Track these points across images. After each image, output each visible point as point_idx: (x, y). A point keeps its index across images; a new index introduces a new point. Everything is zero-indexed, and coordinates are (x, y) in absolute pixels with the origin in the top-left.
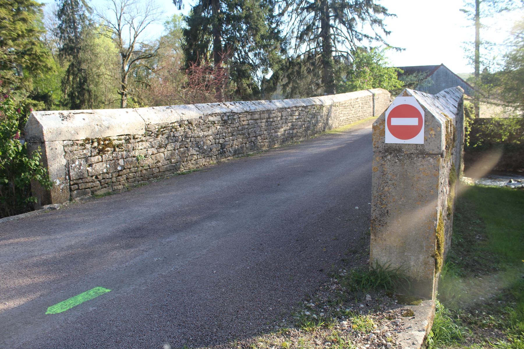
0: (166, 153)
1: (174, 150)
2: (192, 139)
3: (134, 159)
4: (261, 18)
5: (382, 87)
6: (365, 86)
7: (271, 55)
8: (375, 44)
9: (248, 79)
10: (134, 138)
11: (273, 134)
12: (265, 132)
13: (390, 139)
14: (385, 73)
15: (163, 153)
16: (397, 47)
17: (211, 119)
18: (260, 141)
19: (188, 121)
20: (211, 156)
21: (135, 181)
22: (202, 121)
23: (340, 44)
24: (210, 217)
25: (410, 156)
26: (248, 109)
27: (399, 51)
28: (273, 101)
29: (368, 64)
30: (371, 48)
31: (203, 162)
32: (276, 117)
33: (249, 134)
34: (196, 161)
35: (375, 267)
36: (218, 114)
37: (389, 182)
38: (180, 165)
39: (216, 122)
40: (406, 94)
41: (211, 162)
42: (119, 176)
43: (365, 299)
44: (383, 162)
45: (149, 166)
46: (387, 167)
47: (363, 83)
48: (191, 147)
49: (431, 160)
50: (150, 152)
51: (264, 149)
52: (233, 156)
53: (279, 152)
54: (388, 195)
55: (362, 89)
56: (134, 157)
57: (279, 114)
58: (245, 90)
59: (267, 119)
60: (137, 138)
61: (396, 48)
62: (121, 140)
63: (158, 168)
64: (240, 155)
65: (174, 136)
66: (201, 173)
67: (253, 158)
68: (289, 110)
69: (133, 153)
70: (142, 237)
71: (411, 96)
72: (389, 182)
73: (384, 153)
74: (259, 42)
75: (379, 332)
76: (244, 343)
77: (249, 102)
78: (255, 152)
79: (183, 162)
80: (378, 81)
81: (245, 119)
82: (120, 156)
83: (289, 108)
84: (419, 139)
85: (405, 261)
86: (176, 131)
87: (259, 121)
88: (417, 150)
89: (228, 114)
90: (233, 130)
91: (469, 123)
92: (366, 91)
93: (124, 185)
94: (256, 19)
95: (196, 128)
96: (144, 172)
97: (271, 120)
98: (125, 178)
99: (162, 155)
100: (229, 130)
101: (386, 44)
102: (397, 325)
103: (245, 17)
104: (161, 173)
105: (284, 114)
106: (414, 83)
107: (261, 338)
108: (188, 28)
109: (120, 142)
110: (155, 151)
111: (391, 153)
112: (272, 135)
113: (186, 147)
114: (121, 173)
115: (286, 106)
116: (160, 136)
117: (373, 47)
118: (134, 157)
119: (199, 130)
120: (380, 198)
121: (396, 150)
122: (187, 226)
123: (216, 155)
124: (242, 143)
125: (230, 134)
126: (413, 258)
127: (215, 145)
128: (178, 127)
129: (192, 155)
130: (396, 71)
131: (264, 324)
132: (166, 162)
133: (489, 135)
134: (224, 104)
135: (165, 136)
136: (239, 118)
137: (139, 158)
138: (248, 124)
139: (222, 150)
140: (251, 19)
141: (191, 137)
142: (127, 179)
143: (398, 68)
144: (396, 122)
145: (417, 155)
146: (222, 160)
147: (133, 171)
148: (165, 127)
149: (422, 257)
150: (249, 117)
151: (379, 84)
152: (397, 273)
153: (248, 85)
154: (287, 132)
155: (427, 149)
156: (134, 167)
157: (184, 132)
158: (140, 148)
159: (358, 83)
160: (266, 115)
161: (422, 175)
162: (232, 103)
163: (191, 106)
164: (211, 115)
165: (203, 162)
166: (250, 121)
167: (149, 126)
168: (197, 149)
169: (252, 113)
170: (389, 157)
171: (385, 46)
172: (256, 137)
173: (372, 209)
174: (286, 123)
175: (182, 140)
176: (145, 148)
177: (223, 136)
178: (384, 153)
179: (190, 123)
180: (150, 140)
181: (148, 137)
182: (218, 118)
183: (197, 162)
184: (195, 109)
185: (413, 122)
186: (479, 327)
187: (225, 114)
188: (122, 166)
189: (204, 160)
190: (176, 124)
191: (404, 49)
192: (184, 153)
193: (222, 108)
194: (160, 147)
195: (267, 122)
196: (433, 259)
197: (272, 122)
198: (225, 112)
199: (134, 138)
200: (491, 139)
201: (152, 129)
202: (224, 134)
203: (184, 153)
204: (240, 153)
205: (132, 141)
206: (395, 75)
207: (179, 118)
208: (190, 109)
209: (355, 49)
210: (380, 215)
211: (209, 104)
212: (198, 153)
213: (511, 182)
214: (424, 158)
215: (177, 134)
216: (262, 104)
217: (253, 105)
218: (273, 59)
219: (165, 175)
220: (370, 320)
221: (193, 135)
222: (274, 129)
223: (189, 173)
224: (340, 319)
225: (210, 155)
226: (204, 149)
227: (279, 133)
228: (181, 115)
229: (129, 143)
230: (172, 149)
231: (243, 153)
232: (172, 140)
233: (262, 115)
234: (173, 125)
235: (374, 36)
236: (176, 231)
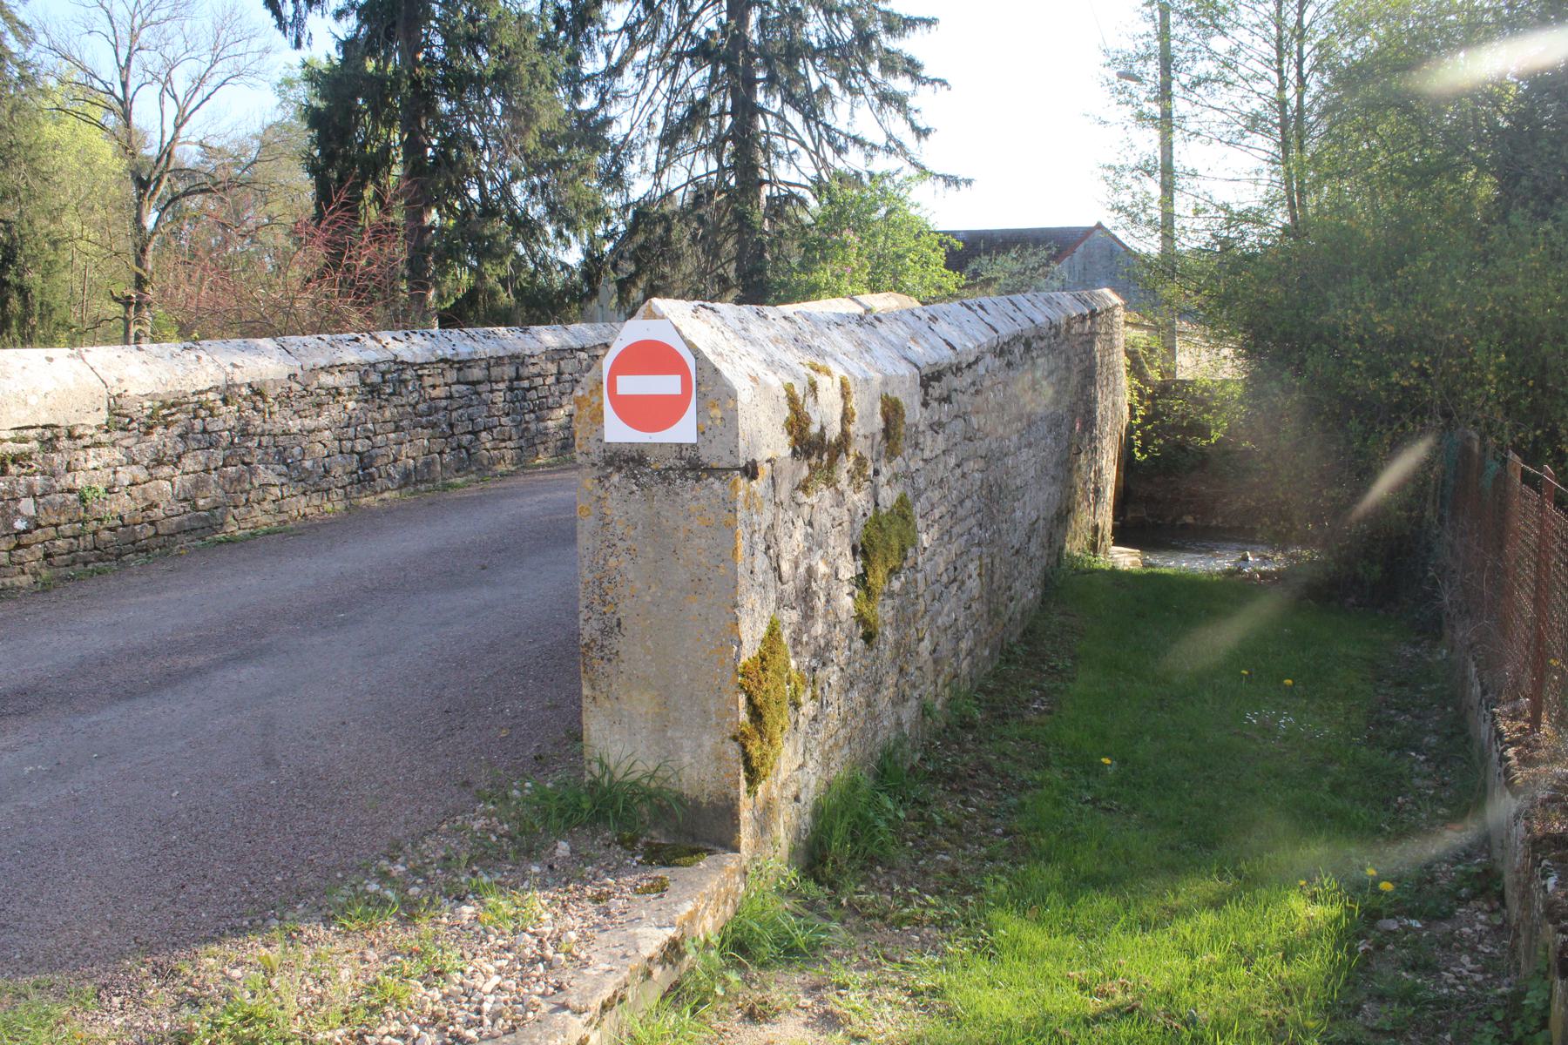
0: (177, 480)
1: (207, 471)
2: (265, 440)
3: (72, 497)
4: (542, 82)
5: (900, 291)
6: (844, 283)
7: (571, 193)
8: (881, 163)
9: (502, 263)
10: (70, 436)
11: (533, 426)
12: (504, 420)
13: (617, 431)
14: (909, 250)
15: (169, 479)
17: (327, 380)
18: (488, 445)
19: (250, 386)
21: (74, 562)
22: (296, 387)
23: (783, 163)
24: (243, 658)
25: (664, 476)
26: (449, 353)
28: (534, 329)
29: (861, 225)
30: (872, 175)
31: (300, 505)
32: (539, 375)
33: (451, 426)
34: (274, 500)
35: (597, 772)
36: (352, 367)
37: (619, 544)
39: (345, 390)
40: (652, 315)
41: (328, 507)
42: (18, 546)
43: (552, 854)
44: (601, 493)
45: (121, 518)
46: (614, 506)
47: (838, 277)
48: (260, 462)
49: (717, 485)
50: (125, 476)
51: (501, 468)
52: (400, 488)
53: (549, 477)
55: (835, 293)
56: (71, 491)
57: (553, 368)
58: (493, 294)
59: (511, 381)
60: (80, 437)
62: (25, 440)
63: (152, 523)
64: (422, 487)
65: (204, 431)
66: (289, 536)
67: (454, 494)
68: (583, 355)
69: (66, 481)
70: (22, 713)
71: (663, 317)
72: (619, 544)
74: (535, 153)
75: (548, 930)
76: (161, 959)
77: (456, 331)
78: (473, 476)
79: (236, 507)
80: (884, 272)
81: (440, 381)
82: (21, 489)
83: (582, 349)
84: (684, 431)
85: (669, 752)
87: (481, 388)
89: (383, 367)
91: (1141, 394)
92: (846, 301)
93: (35, 574)
94: (526, 83)
95: (276, 408)
96: (106, 535)
97: (526, 384)
98: (40, 554)
99: (166, 487)
100: (388, 414)
101: (915, 165)
102: (607, 914)
103: (494, 78)
104: (161, 540)
105: (568, 366)
106: (995, 279)
107: (215, 948)
108: (318, 103)
109: (25, 447)
110: (142, 475)
111: (619, 469)
112: (527, 429)
113: (244, 463)
114: (25, 539)
115: (575, 344)
116: (160, 429)
117: (878, 172)
118: (71, 491)
119: (288, 412)
120: (600, 586)
121: (633, 459)
122: (170, 680)
123: (343, 487)
124: (430, 452)
125: (391, 426)
126: (687, 744)
127: (339, 458)
128: (219, 403)
129: (265, 486)
130: (941, 243)
131: (240, 916)
132: (178, 507)
133: (1176, 428)
134: (373, 338)
135: (175, 430)
136: (420, 377)
137: (89, 495)
138: (450, 397)
139: (365, 472)
140: (512, 84)
142: (47, 556)
143: (946, 233)
144: (629, 385)
145: (682, 474)
146: (364, 501)
147: (69, 533)
148: (173, 405)
149: (708, 742)
150: (452, 376)
152: (653, 785)
153: (503, 281)
155: (708, 456)
156: (70, 521)
157: (239, 419)
158: (91, 464)
159: (823, 275)
160: (509, 371)
162: (400, 334)
163: (266, 343)
164: (328, 369)
165: (300, 505)
166: (454, 388)
167: (120, 402)
168: (282, 468)
169: (462, 365)
170: (616, 478)
171: (914, 172)
172: (475, 433)
173: (582, 617)
175: (232, 443)
176: (109, 466)
178: (603, 469)
179: (257, 392)
180: (125, 443)
181: (118, 434)
182: (352, 378)
185: (669, 385)
186: (889, 926)
187: (373, 365)
188: (29, 519)
189: (304, 500)
190: (211, 396)
191: (969, 182)
192: (239, 479)
193: (364, 348)
194: (159, 462)
195: (511, 389)
196: (735, 745)
197: (529, 390)
198: (372, 360)
199: (70, 436)
200: (1183, 439)
201: (133, 409)
202: (370, 426)
204: (421, 482)
205: (64, 443)
206: (939, 257)
207: (223, 377)
208: (259, 352)
209: (826, 178)
210: (602, 632)
211: (326, 337)
212: (284, 480)
213: (1245, 559)
214: (698, 479)
217: (469, 342)
218: (577, 205)
219: (175, 544)
220: (538, 902)
221: (267, 427)
222: (533, 411)
224: (461, 900)
225: (325, 485)
226: (305, 469)
227: (550, 424)
228: (229, 369)
229: (55, 449)
230: (197, 468)
231: (434, 481)
232: (199, 441)
233: (495, 372)
235: (881, 140)
236: (130, 695)
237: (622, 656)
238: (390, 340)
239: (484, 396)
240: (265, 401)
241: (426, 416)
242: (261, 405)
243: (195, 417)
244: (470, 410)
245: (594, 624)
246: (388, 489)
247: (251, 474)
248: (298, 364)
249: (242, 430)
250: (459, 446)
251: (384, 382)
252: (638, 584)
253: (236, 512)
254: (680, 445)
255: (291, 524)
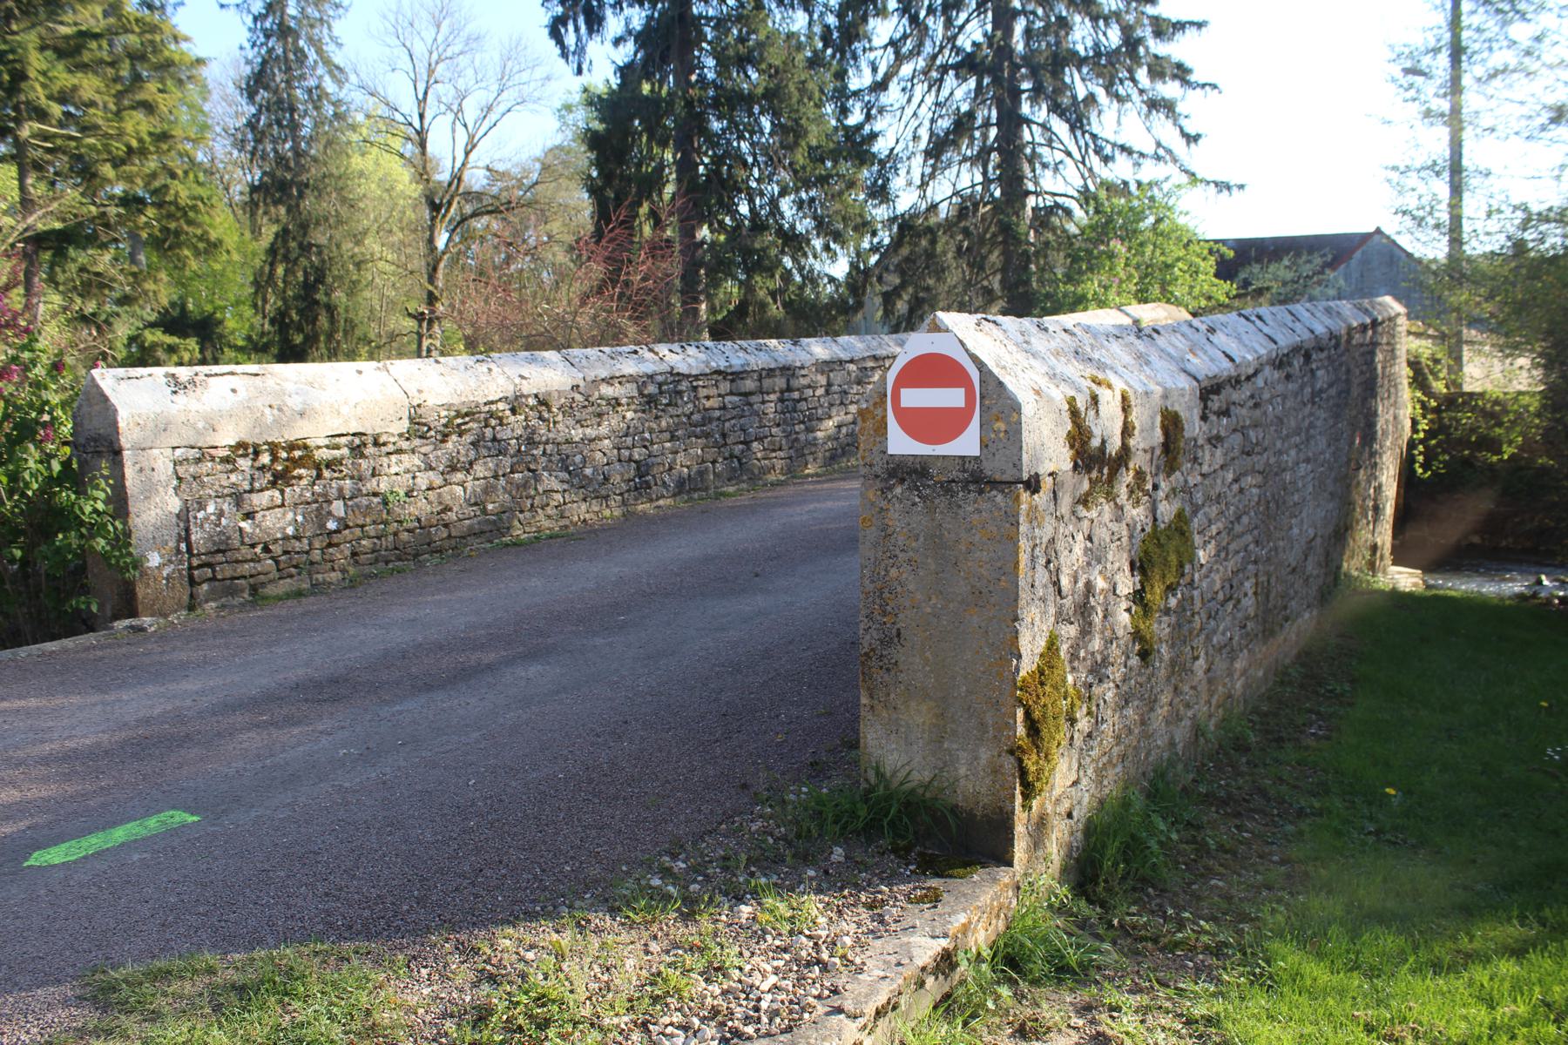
0: (469, 485)
1: (496, 477)
2: (549, 448)
3: (376, 500)
4: (810, 99)
5: (1168, 301)
6: (1112, 295)
7: (838, 206)
8: (1150, 171)
9: (773, 276)
10: (376, 444)
11: (802, 437)
12: (774, 430)
13: (900, 443)
14: (1178, 259)
15: (462, 484)
16: (1219, 179)
17: (607, 390)
19: (536, 396)
20: (606, 497)
21: (377, 561)
22: (578, 397)
23: (1048, 173)
24: (531, 656)
25: (947, 488)
26: (722, 364)
27: (1225, 192)
28: (805, 341)
29: (1129, 234)
30: (1139, 184)
31: (581, 511)
32: (809, 387)
33: (724, 436)
34: (558, 505)
35: (873, 780)
36: (631, 379)
37: (901, 555)
38: (510, 520)
39: (624, 401)
40: (937, 328)
41: (607, 513)
42: (330, 545)
43: (827, 859)
44: (883, 504)
45: (419, 520)
46: (895, 517)
47: (1106, 288)
49: (999, 498)
50: (423, 481)
51: (772, 477)
52: (674, 495)
54: (899, 589)
55: (1102, 304)
56: (375, 494)
57: (822, 380)
58: (763, 306)
59: (782, 392)
60: (384, 444)
61: (1216, 184)
62: (337, 447)
63: (446, 526)
64: (696, 496)
65: (494, 439)
67: (728, 502)
68: (852, 367)
69: (371, 485)
70: (335, 700)
71: (947, 330)
72: (901, 555)
73: (886, 480)
74: (804, 168)
75: (824, 933)
76: (463, 937)
77: (729, 343)
78: (744, 486)
79: (522, 512)
80: (1153, 282)
81: (713, 391)
82: (333, 492)
83: (852, 361)
84: (967, 444)
85: (945, 763)
86: (501, 424)
87: (754, 399)
88: (964, 471)
89: (660, 378)
90: (677, 425)
91: (1424, 406)
92: (1114, 312)
93: (343, 571)
94: (794, 100)
95: (560, 418)
96: (405, 536)
97: (796, 395)
98: (348, 553)
99: (458, 492)
100: (664, 424)
101: (1186, 172)
102: (882, 922)
103: (764, 96)
104: (453, 542)
105: (837, 377)
106: (1268, 289)
107: (511, 931)
108: (597, 126)
109: (337, 453)
110: (438, 481)
111: (902, 481)
112: (797, 440)
113: (529, 470)
114: (336, 539)
115: (844, 356)
116: (454, 438)
117: (1145, 180)
118: (375, 494)
119: (571, 422)
121: (915, 471)
122: (464, 675)
124: (703, 462)
125: (667, 435)
126: (963, 755)
127: (617, 466)
128: (508, 413)
130: (1211, 252)
131: (533, 901)
132: (470, 511)
133: (1463, 442)
134: (651, 350)
135: (468, 438)
136: (695, 388)
137: (391, 498)
138: (723, 408)
139: (642, 478)
140: (781, 102)
141: (547, 443)
142: (354, 554)
143: (1216, 242)
144: (914, 398)
145: (966, 485)
146: (640, 507)
147: (372, 533)
148: (467, 414)
149: (985, 755)
150: (725, 387)
151: (1163, 290)
152: (928, 795)
153: (773, 294)
154: (844, 430)
155: (989, 469)
156: (374, 522)
157: (525, 428)
158: (394, 470)
159: (1091, 286)
160: (780, 383)
161: (977, 538)
162: (676, 347)
163: (551, 355)
164: (608, 381)
165: (581, 511)
166: (728, 399)
167: (419, 411)
169: (735, 376)
170: (898, 490)
171: (1184, 179)
172: (747, 443)
173: (862, 626)
174: (842, 403)
176: (408, 471)
177: (645, 439)
178: (886, 480)
179: (543, 402)
180: (423, 450)
181: (417, 442)
182: (631, 389)
183: (562, 512)
184: (561, 365)
185: (953, 398)
186: (1162, 950)
187: (651, 377)
188: (339, 520)
189: (584, 507)
190: (501, 406)
191: (1241, 187)
192: (525, 485)
193: (642, 360)
194: (453, 468)
195: (781, 400)
196: (1012, 759)
197: (799, 401)
198: (649, 372)
199: (376, 444)
200: (1471, 455)
201: (430, 418)
202: (647, 435)
203: (525, 485)
204: (695, 490)
205: (370, 450)
206: (1209, 266)
207: (512, 388)
208: (545, 364)
209: (1092, 188)
211: (607, 349)
212: (566, 486)
213: (1539, 582)
214: (981, 492)
215: (503, 434)
216: (769, 351)
217: (741, 354)
218: (844, 219)
219: (466, 545)
220: (812, 905)
221: (551, 435)
222: (803, 422)
223: (537, 544)
224: (740, 900)
225: (603, 492)
227: (819, 434)
228: (517, 380)
229: (363, 456)
230: (487, 474)
231: (707, 489)
233: (767, 383)
234: (494, 407)
235: (1149, 149)
236: (429, 688)
240: (550, 411)
241: (701, 426)
242: (546, 415)
245: (875, 634)
249: (528, 439)
251: (661, 393)
252: (919, 596)
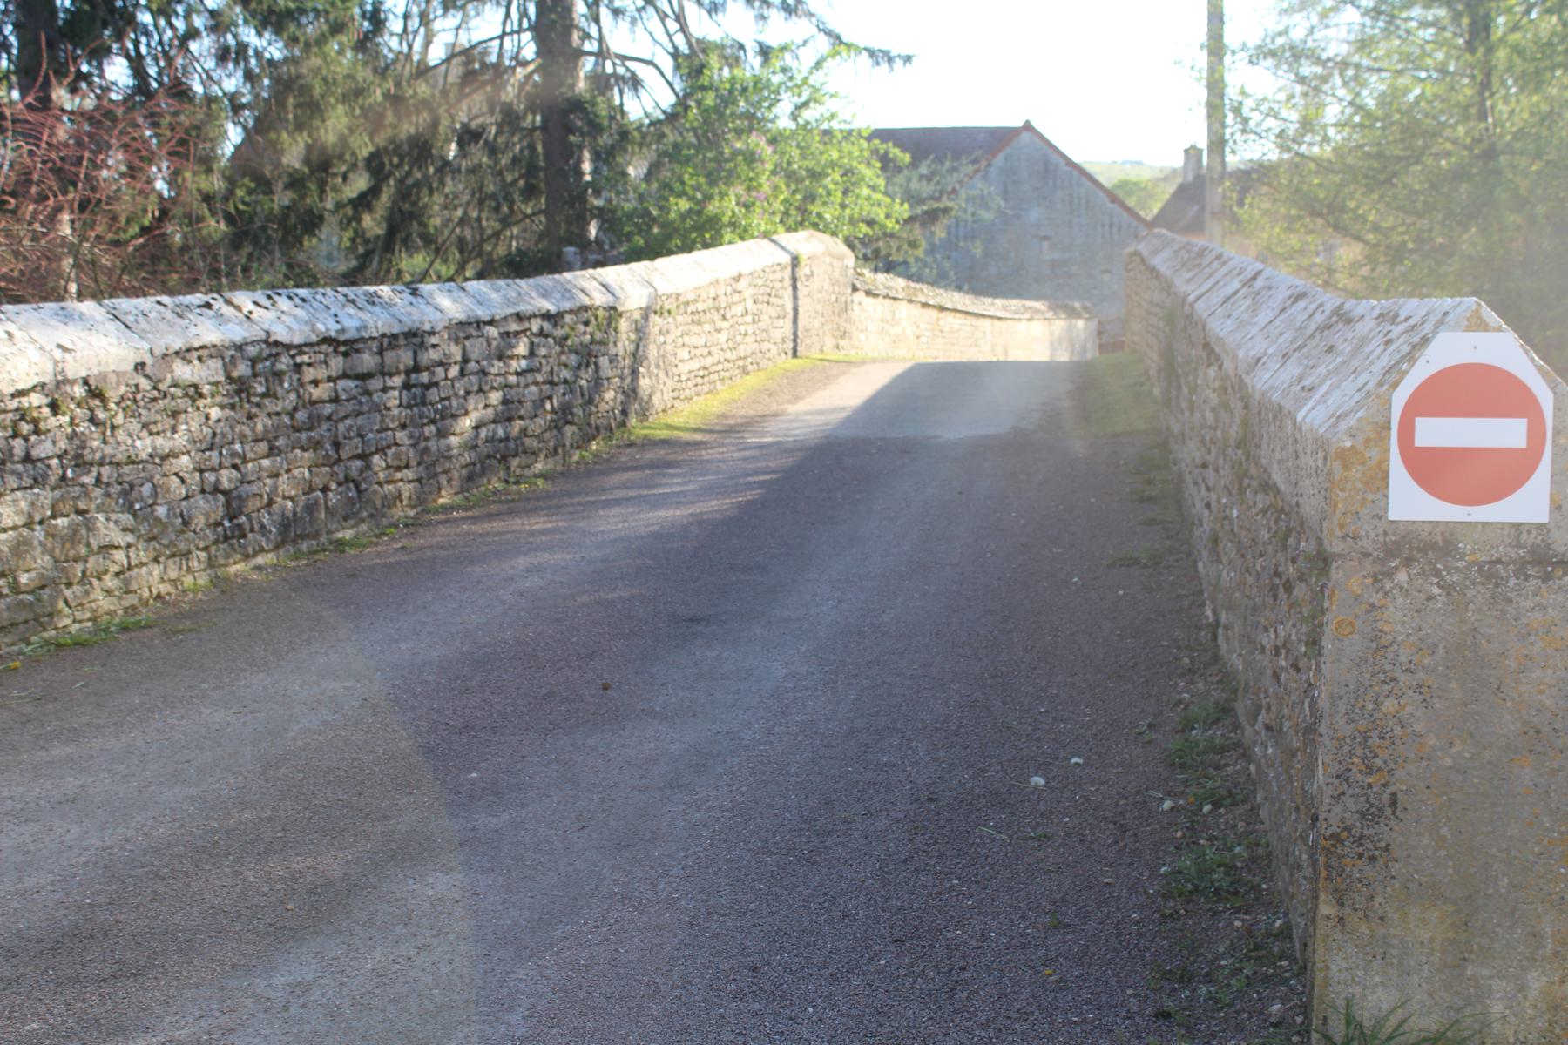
1: (29, 525)
5: (815, 226)
7: (316, 61)
11: (433, 445)
12: (401, 436)
14: (833, 165)
16: (876, 47)
18: (382, 476)
19: (86, 382)
20: (186, 554)
22: (145, 384)
23: (624, 24)
27: (884, 66)
32: (441, 364)
33: (337, 445)
34: (130, 574)
36: (215, 351)
37: (1403, 678)
38: (53, 599)
39: (206, 389)
47: (747, 206)
48: (98, 510)
52: (277, 547)
53: (477, 528)
54: (1398, 731)
59: (408, 373)
61: (872, 53)
64: (304, 547)
65: (27, 459)
68: (493, 332)
72: (1403, 678)
73: (1383, 561)
78: (364, 527)
79: (69, 585)
81: (322, 373)
83: (491, 322)
85: (1468, 1002)
86: (37, 432)
87: (375, 384)
88: (1519, 546)
89: (252, 351)
90: (276, 428)
97: (425, 377)
100: (260, 427)
101: (829, 33)
105: (476, 348)
106: (946, 211)
111: (1408, 562)
112: (426, 450)
115: (483, 313)
117: (773, 41)
120: (1364, 744)
121: (1433, 546)
123: (206, 549)
124: (311, 490)
125: (263, 447)
126: (1499, 985)
128: (46, 411)
129: (106, 549)
134: (228, 302)
138: (335, 400)
141: (101, 464)
144: (1433, 432)
146: (233, 569)
150: (337, 364)
151: (803, 211)
154: (483, 433)
159: (728, 204)
160: (405, 357)
161: (1537, 648)
162: (259, 295)
165: (153, 579)
166: (342, 384)
168: (126, 519)
170: (1402, 577)
172: (364, 457)
174: (480, 390)
175: (63, 478)
177: (234, 454)
183: (127, 583)
184: (113, 326)
187: (240, 348)
189: (157, 571)
191: (908, 59)
195: (407, 386)
197: (427, 387)
198: (238, 339)
202: (237, 447)
203: (73, 537)
204: (304, 537)
207: (50, 367)
210: (1363, 815)
212: (130, 538)
214: (1546, 578)
215: (43, 449)
216: (387, 306)
217: (351, 310)
218: (325, 80)
221: (108, 450)
222: (433, 422)
223: (98, 643)
225: (182, 546)
226: (158, 519)
227: (454, 440)
228: (58, 354)
232: (19, 476)
233: (390, 356)
234: (25, 401)
237: (1396, 852)
238: (252, 307)
239: (375, 397)
240: (106, 409)
241: (308, 425)
242: (101, 415)
243: (15, 435)
244: (360, 420)
245: (1350, 803)
246: (262, 550)
247: (89, 530)
248: (146, 346)
249: (78, 456)
250: (347, 479)
251: (255, 375)
252: (1432, 741)
253: (68, 593)
254: (1517, 526)
255: (144, 615)
